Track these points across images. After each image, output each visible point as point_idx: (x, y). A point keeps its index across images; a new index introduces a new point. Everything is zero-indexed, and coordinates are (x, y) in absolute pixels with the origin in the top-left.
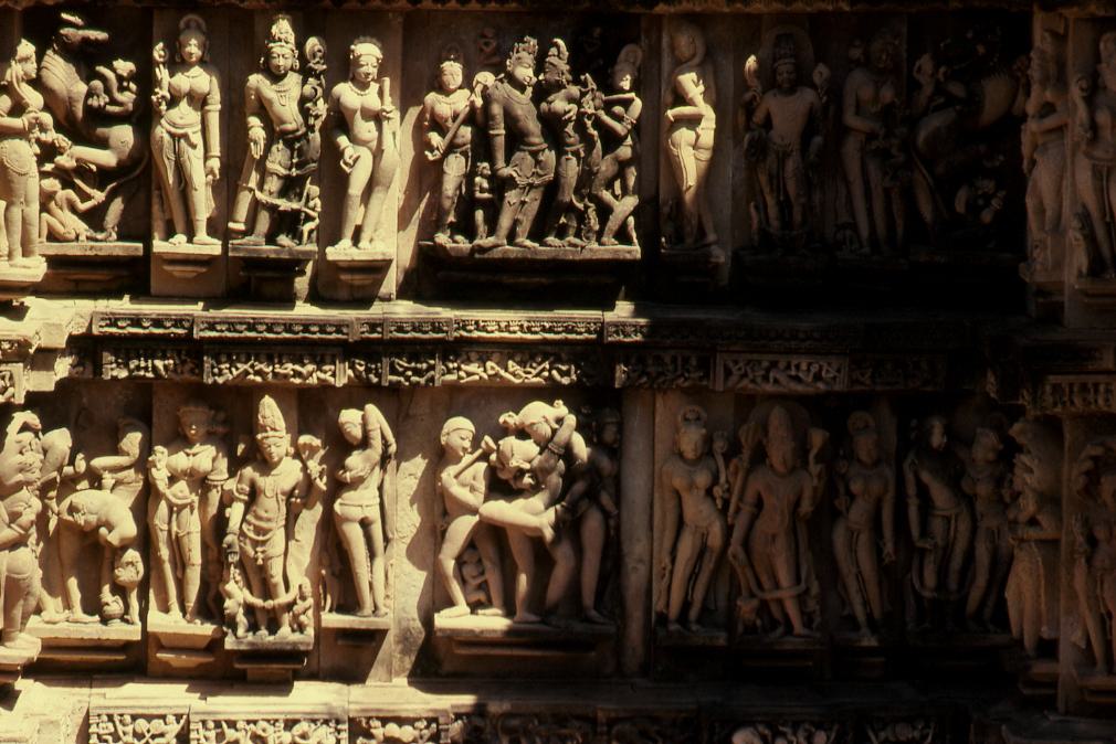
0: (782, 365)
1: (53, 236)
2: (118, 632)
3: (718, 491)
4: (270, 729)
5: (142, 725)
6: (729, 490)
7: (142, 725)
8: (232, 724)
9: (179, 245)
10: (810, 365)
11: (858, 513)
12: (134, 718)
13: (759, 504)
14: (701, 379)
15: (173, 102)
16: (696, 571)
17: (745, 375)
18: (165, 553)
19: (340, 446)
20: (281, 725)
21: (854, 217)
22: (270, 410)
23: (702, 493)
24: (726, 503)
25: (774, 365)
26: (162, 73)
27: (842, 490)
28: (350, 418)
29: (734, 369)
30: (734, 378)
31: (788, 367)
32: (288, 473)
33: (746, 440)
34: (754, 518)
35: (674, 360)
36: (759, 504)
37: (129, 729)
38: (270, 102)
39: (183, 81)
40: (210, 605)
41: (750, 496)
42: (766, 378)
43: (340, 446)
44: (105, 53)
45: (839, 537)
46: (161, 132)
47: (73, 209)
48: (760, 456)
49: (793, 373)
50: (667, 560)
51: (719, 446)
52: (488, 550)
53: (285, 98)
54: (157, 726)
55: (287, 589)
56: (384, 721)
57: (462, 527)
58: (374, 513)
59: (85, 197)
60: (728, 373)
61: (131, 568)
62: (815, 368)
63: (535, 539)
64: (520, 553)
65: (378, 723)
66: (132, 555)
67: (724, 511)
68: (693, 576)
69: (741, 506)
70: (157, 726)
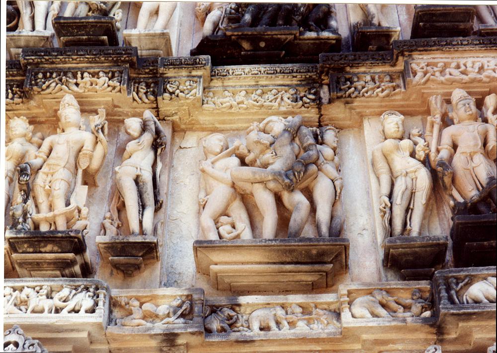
10: (473, 63)
13: (455, 147)
16: (411, 207)
17: (425, 74)
23: (408, 154)
25: (446, 66)
30: (420, 74)
31: (458, 67)
33: (436, 103)
36: (455, 147)
49: (463, 68)
55: (68, 204)
57: (220, 194)
58: (147, 176)
62: (478, 65)
65: (137, 303)
69: (439, 147)
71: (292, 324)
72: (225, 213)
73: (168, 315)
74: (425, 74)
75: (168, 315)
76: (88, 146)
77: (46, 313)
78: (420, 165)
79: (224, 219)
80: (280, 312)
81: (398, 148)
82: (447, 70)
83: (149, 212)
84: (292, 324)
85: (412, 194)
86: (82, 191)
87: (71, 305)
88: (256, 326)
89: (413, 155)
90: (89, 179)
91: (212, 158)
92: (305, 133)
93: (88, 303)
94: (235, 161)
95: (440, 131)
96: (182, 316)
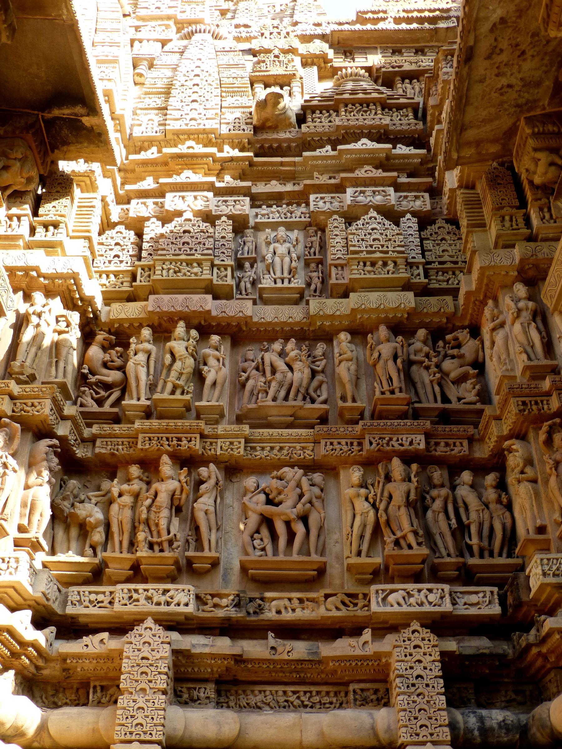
0: (395, 439)
1: (82, 405)
3: (370, 496)
4: (155, 593)
5: (93, 597)
6: (376, 495)
7: (93, 597)
8: (136, 591)
11: (438, 505)
12: (90, 593)
14: (360, 451)
20: (160, 592)
21: (419, 397)
22: (165, 458)
24: (375, 501)
25: (391, 439)
27: (428, 497)
29: (373, 441)
30: (374, 445)
31: (398, 440)
32: (173, 485)
34: (389, 503)
35: (347, 443)
36: (390, 497)
37: (87, 599)
38: (174, 348)
39: (141, 346)
41: (386, 494)
42: (388, 444)
44: (112, 346)
45: (429, 514)
47: (92, 398)
48: (388, 478)
49: (400, 442)
50: (350, 529)
54: (101, 597)
55: (169, 533)
56: (213, 596)
57: (254, 519)
59: (97, 393)
60: (371, 443)
61: (98, 536)
62: (409, 440)
65: (209, 597)
66: (101, 529)
67: (374, 505)
68: (362, 537)
70: (101, 597)
71: (294, 610)
72: (258, 531)
73: (227, 606)
74: (378, 444)
75: (227, 606)
76: (178, 492)
77: (162, 606)
78: (370, 508)
79: (256, 535)
80: (287, 602)
81: (358, 495)
82: (391, 443)
83: (214, 531)
84: (294, 610)
85: (365, 526)
86: (176, 521)
87: (176, 601)
88: (274, 610)
89: (367, 499)
90: (178, 510)
91: (250, 495)
92: (315, 349)
93: (184, 600)
94: (262, 497)
95: (384, 486)
96: (235, 606)
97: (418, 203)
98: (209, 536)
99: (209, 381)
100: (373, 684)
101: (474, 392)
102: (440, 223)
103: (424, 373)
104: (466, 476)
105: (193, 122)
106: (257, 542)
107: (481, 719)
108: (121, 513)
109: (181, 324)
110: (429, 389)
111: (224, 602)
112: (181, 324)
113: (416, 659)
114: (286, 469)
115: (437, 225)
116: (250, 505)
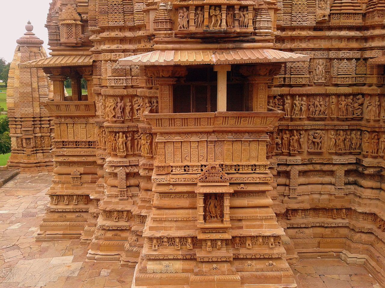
2: (279, 152)
9: (286, 116)
11: (348, 140)
15: (287, 103)
18: (284, 144)
19: (300, 134)
22: (295, 132)
26: (286, 101)
28: (301, 132)
32: (296, 137)
40: (289, 150)
43: (300, 134)
46: (285, 106)
51: (335, 134)
52: (312, 144)
53: (297, 103)
57: (310, 142)
63: (318, 143)
64: (316, 144)
67: (335, 140)
70: (284, 160)
97: (358, 54)
98: (303, 146)
99: (303, 111)
100: (332, 173)
101: (360, 112)
102: (362, 60)
103: (350, 108)
104: (354, 132)
105: (299, 23)
106: (311, 146)
107: (349, 180)
108: (285, 141)
109: (297, 97)
110: (350, 112)
111: (306, 160)
112: (297, 97)
113: (340, 171)
114: (318, 131)
115: (361, 61)
116: (310, 138)
